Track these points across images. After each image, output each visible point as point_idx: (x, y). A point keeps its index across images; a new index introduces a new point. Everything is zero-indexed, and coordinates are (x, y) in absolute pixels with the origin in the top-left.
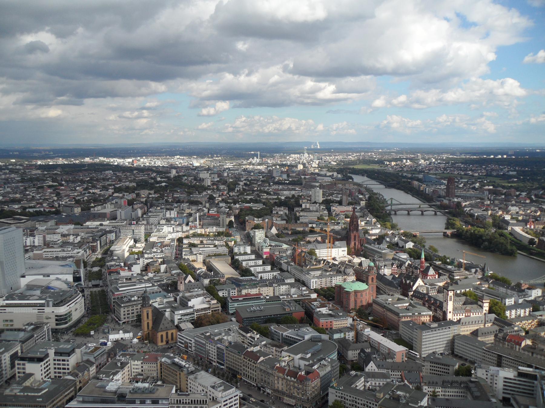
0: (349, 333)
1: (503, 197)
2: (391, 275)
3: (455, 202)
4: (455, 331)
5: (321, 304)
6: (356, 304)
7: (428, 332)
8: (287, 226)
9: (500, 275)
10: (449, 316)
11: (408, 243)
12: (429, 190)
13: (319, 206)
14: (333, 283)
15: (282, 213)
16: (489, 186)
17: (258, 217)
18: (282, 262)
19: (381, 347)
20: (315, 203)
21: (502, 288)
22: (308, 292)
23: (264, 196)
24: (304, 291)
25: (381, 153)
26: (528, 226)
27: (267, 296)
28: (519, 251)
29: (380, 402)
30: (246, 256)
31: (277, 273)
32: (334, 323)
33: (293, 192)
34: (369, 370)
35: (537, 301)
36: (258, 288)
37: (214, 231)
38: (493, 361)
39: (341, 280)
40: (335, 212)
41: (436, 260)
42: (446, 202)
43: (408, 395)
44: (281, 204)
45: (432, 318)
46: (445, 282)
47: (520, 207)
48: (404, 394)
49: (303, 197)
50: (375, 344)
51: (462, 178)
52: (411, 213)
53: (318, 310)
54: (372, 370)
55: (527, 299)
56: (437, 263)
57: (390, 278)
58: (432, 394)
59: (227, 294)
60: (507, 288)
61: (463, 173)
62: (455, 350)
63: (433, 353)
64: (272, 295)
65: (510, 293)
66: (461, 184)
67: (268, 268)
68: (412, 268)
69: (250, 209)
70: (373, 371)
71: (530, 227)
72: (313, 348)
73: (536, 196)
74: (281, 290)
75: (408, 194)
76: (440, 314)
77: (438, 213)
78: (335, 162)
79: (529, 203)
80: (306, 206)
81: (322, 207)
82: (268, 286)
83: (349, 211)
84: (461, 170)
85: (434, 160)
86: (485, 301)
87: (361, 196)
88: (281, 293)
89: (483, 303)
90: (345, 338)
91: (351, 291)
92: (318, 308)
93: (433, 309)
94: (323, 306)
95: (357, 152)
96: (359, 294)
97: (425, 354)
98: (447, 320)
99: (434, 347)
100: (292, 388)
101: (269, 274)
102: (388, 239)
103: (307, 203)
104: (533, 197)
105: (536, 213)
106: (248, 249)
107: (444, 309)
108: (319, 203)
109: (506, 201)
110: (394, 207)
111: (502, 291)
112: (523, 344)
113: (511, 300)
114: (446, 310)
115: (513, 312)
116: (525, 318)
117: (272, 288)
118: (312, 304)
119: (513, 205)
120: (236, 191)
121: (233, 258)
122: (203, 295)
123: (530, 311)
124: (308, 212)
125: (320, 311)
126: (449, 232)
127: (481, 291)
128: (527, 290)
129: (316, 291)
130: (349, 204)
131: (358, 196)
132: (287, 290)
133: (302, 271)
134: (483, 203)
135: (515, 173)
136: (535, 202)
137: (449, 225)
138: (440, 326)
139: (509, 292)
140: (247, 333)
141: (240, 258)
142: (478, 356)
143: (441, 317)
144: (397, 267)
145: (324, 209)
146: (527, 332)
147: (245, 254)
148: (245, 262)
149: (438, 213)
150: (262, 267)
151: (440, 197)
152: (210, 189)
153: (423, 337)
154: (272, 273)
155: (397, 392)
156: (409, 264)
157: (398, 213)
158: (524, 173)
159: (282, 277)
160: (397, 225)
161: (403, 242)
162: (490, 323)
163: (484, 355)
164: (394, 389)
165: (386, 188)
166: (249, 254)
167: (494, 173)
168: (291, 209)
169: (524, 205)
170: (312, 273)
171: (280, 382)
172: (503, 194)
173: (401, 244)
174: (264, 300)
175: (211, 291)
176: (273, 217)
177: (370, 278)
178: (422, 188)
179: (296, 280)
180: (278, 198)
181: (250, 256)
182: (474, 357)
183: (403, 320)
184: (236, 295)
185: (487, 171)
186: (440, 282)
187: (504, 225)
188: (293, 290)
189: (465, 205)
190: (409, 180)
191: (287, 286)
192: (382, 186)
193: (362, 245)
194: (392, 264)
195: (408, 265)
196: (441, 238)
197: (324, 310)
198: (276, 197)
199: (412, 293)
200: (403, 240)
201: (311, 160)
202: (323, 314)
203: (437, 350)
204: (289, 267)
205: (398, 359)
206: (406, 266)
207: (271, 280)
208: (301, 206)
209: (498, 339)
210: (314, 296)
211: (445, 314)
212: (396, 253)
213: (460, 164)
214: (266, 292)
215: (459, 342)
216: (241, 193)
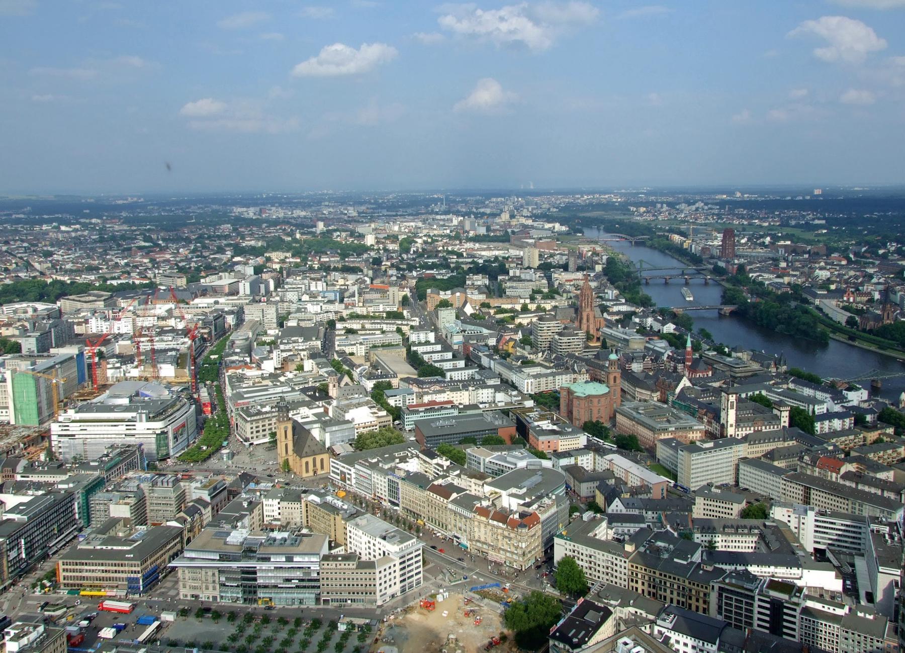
0: (583, 458)
1: (806, 256)
2: (643, 371)
3: (736, 264)
4: (740, 454)
5: (541, 415)
6: (591, 414)
7: (699, 455)
8: (487, 301)
9: (804, 370)
10: (731, 431)
12: (696, 248)
14: (557, 384)
15: (479, 283)
16: (785, 241)
17: (445, 290)
18: (480, 354)
19: (630, 478)
20: (529, 268)
21: (808, 389)
24: (515, 396)
25: (622, 195)
26: (845, 299)
28: (831, 335)
29: (630, 558)
30: (428, 347)
31: (473, 371)
32: (560, 443)
34: (613, 510)
35: (861, 408)
37: (381, 310)
38: (797, 496)
39: (568, 380)
40: (558, 281)
41: (709, 350)
42: (722, 264)
43: (671, 546)
44: (477, 269)
45: (704, 434)
47: (832, 270)
48: (667, 545)
49: (510, 260)
50: (621, 473)
51: (744, 230)
53: (536, 424)
54: (617, 511)
55: (845, 405)
56: (710, 354)
57: (641, 377)
58: (707, 545)
59: (401, 402)
60: (816, 389)
61: (746, 223)
62: (740, 480)
63: (708, 485)
66: (743, 238)
67: (461, 364)
69: (433, 278)
70: (619, 512)
71: (849, 299)
72: (529, 480)
73: (855, 254)
74: (480, 395)
75: (666, 254)
76: (716, 429)
78: (557, 208)
80: (514, 273)
81: (538, 274)
83: (579, 279)
84: (743, 218)
89: (781, 411)
90: (576, 464)
92: (537, 421)
93: (705, 420)
94: (542, 418)
95: (588, 194)
96: (595, 401)
97: (695, 487)
98: (727, 436)
99: (709, 477)
100: (500, 538)
101: (463, 372)
102: (637, 320)
103: (517, 268)
104: (851, 256)
105: (857, 280)
106: (431, 337)
107: (722, 421)
108: (534, 269)
109: (810, 262)
112: (843, 470)
113: (822, 407)
114: (725, 422)
115: (827, 423)
116: (843, 433)
118: (528, 416)
119: (821, 269)
120: (412, 252)
121: (409, 350)
124: (519, 281)
125: (539, 426)
126: (727, 309)
128: (846, 392)
129: (531, 397)
130: (579, 269)
133: (510, 368)
134: (777, 265)
135: (823, 222)
136: (855, 262)
137: (727, 299)
138: (717, 446)
139: (819, 395)
140: (432, 457)
141: (420, 349)
142: (774, 488)
143: (718, 433)
144: (651, 359)
146: (847, 454)
147: (427, 343)
148: (427, 355)
150: (452, 363)
151: (712, 257)
152: (373, 249)
153: (692, 462)
154: (467, 372)
155: (656, 542)
156: (669, 355)
158: (837, 222)
160: (650, 300)
162: (791, 440)
163: (784, 487)
164: (651, 539)
167: (793, 223)
168: (493, 277)
169: (838, 268)
170: (527, 370)
171: (482, 529)
172: (806, 253)
175: (379, 396)
176: (466, 289)
177: (611, 377)
178: (685, 246)
179: (502, 380)
182: (768, 491)
183: (662, 437)
184: (415, 403)
185: (781, 218)
186: (715, 381)
187: (809, 298)
188: (501, 397)
189: (751, 269)
190: (666, 234)
191: (491, 391)
193: (598, 330)
194: (644, 357)
195: (668, 358)
197: (546, 425)
198: (470, 260)
200: (658, 321)
201: (522, 206)
202: (543, 430)
203: (713, 481)
204: (492, 362)
205: (656, 494)
206: (665, 359)
207: (465, 381)
208: (508, 273)
209: (804, 465)
210: (529, 403)
211: (723, 427)
212: (649, 339)
214: (459, 399)
215: (746, 468)
216: (419, 255)
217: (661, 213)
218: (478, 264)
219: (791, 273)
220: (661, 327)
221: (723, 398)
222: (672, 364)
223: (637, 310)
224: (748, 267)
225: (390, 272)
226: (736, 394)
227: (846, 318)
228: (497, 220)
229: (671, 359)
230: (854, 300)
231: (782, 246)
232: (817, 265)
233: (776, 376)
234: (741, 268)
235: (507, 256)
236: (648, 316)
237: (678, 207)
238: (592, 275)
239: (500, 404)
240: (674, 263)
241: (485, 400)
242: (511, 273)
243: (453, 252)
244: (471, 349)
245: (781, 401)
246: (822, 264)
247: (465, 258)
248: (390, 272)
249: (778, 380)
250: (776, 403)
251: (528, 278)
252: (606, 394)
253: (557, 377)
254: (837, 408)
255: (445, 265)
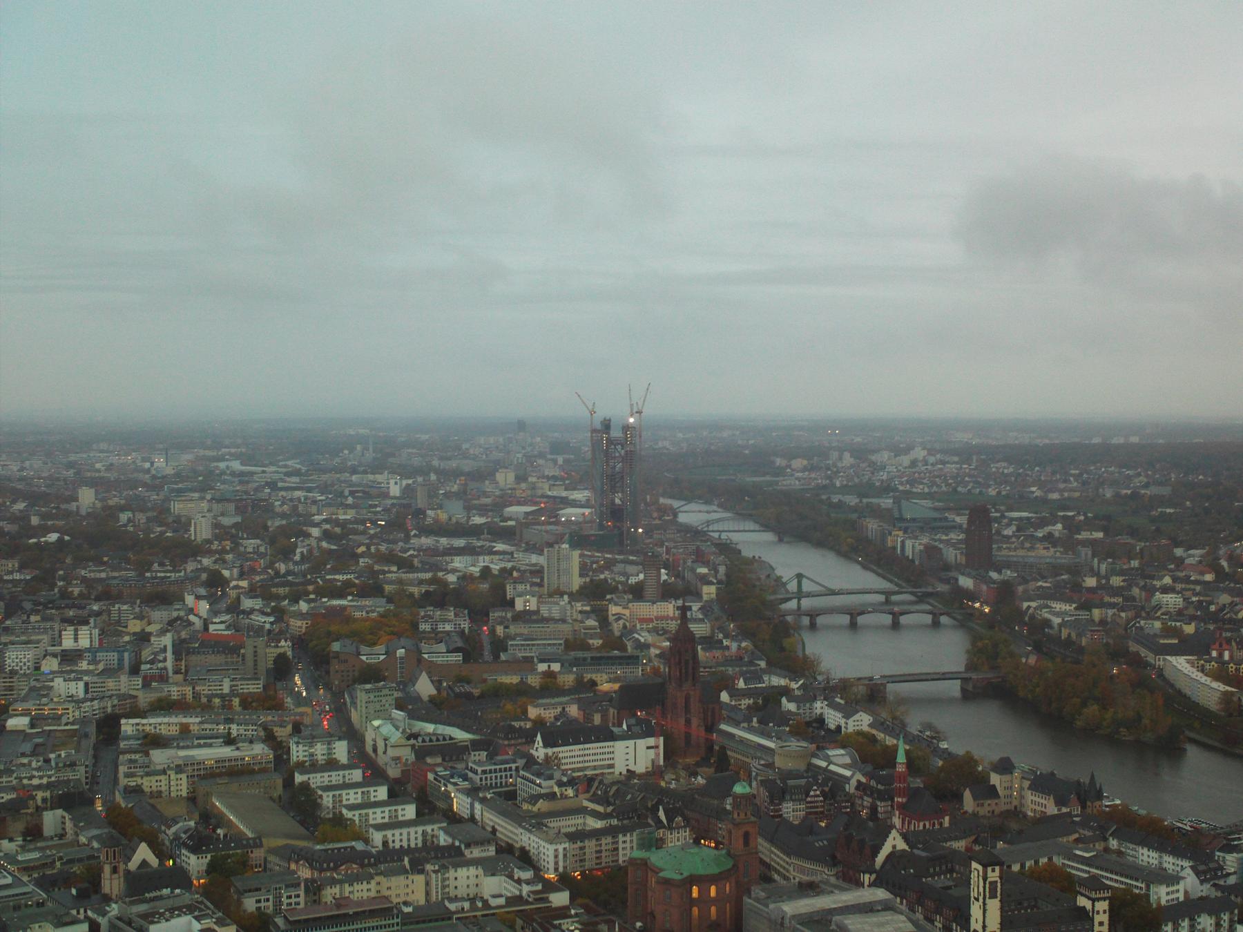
1: (1135, 563)
3: (994, 582)
11: (857, 717)
13: (569, 602)
14: (621, 852)
15: (448, 627)
21: (1145, 851)
22: (539, 887)
23: (390, 572)
27: (406, 903)
30: (333, 774)
31: (435, 827)
33: (483, 561)
36: (378, 879)
40: (621, 622)
42: (966, 582)
46: (973, 838)
47: (1188, 594)
49: (515, 574)
52: (861, 620)
55: (1222, 882)
59: (270, 903)
64: (422, 902)
65: (1171, 867)
66: (1008, 525)
67: (409, 811)
68: (871, 796)
71: (1221, 655)
74: (452, 883)
77: (944, 619)
79: (1214, 582)
81: (579, 606)
82: (406, 872)
83: (667, 618)
85: (924, 453)
86: (1098, 896)
87: (703, 570)
88: (452, 895)
91: (678, 877)
101: (412, 830)
102: (792, 707)
108: (571, 595)
109: (1145, 577)
110: (806, 603)
111: (1145, 858)
113: (1174, 888)
117: (420, 879)
119: (1165, 590)
120: (297, 558)
122: (190, 909)
123: (1231, 921)
124: (537, 621)
127: (1082, 863)
130: (667, 593)
131: (693, 570)
132: (473, 881)
133: (519, 818)
135: (1166, 491)
141: (316, 780)
144: (823, 794)
145: (586, 612)
147: (332, 765)
148: (331, 794)
149: (944, 619)
150: (387, 809)
151: (947, 567)
152: (210, 552)
154: (420, 829)
156: (859, 781)
157: (820, 620)
159: (454, 838)
161: (839, 715)
165: (781, 540)
166: (344, 767)
168: (479, 614)
169: (1198, 588)
173: (833, 718)
174: (396, 920)
179: (499, 850)
180: (434, 581)
181: (347, 772)
186: (957, 839)
191: (472, 871)
192: (769, 537)
195: (857, 788)
196: (951, 701)
198: (428, 575)
199: (874, 876)
204: (478, 806)
206: (852, 791)
207: (416, 849)
208: (511, 603)
213: (1004, 464)
216: (316, 562)
217: (838, 472)
218: (445, 584)
219: (1107, 599)
220: (842, 722)
221: (974, 875)
222: (867, 801)
223: (794, 685)
224: (1020, 589)
225: (247, 603)
226: (1001, 864)
227: (1218, 694)
228: (488, 486)
229: (864, 790)
230: (1231, 657)
231: (1084, 543)
232: (1158, 584)
233: (1084, 824)
234: (1005, 593)
235: (509, 565)
236: (815, 699)
237: (873, 458)
238: (695, 607)
239: (494, 902)
240: (871, 580)
241: (461, 892)
242: (519, 605)
243: (390, 558)
244: (431, 776)
245: (1094, 878)
246: (1167, 580)
247: (417, 570)
248: (247, 603)
249: (1088, 833)
250: (1083, 883)
251: (556, 615)
252: (729, 870)
253: (621, 838)
254: (1205, 890)
255: (372, 589)
